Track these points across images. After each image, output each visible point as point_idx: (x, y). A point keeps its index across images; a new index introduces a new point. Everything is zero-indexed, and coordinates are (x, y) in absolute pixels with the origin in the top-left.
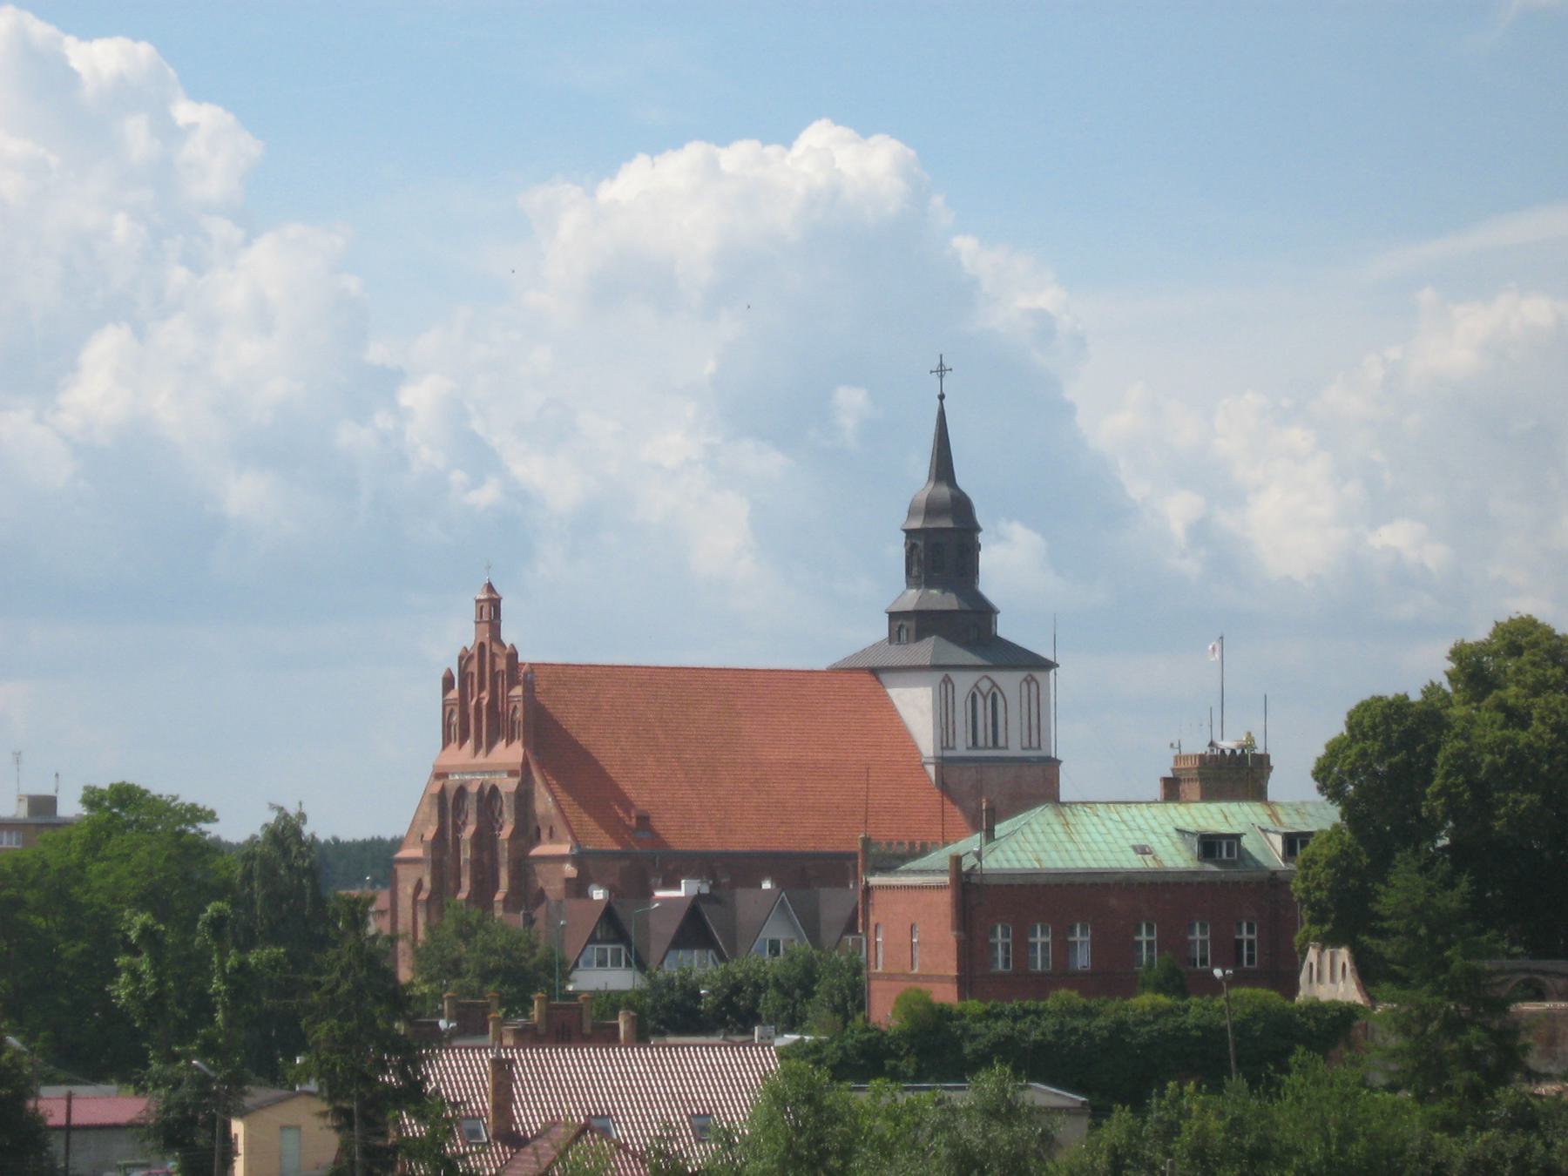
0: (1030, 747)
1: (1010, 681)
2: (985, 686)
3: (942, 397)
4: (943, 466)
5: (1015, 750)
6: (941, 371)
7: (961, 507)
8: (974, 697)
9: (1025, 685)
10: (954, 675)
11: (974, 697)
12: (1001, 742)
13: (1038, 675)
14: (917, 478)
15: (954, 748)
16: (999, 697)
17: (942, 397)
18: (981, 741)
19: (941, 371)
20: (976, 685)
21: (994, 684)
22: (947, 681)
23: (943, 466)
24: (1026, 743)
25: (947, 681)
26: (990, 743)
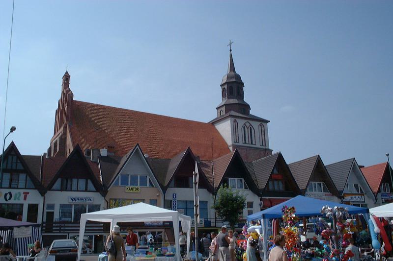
0: (262, 145)
1: (255, 125)
2: (248, 125)
3: (231, 50)
5: (258, 146)
6: (230, 44)
7: (238, 77)
8: (244, 129)
9: (260, 127)
10: (238, 120)
12: (254, 143)
14: (226, 70)
17: (231, 50)
18: (247, 142)
19: (230, 44)
20: (245, 124)
21: (251, 125)
24: (261, 144)
25: (235, 121)
26: (250, 143)
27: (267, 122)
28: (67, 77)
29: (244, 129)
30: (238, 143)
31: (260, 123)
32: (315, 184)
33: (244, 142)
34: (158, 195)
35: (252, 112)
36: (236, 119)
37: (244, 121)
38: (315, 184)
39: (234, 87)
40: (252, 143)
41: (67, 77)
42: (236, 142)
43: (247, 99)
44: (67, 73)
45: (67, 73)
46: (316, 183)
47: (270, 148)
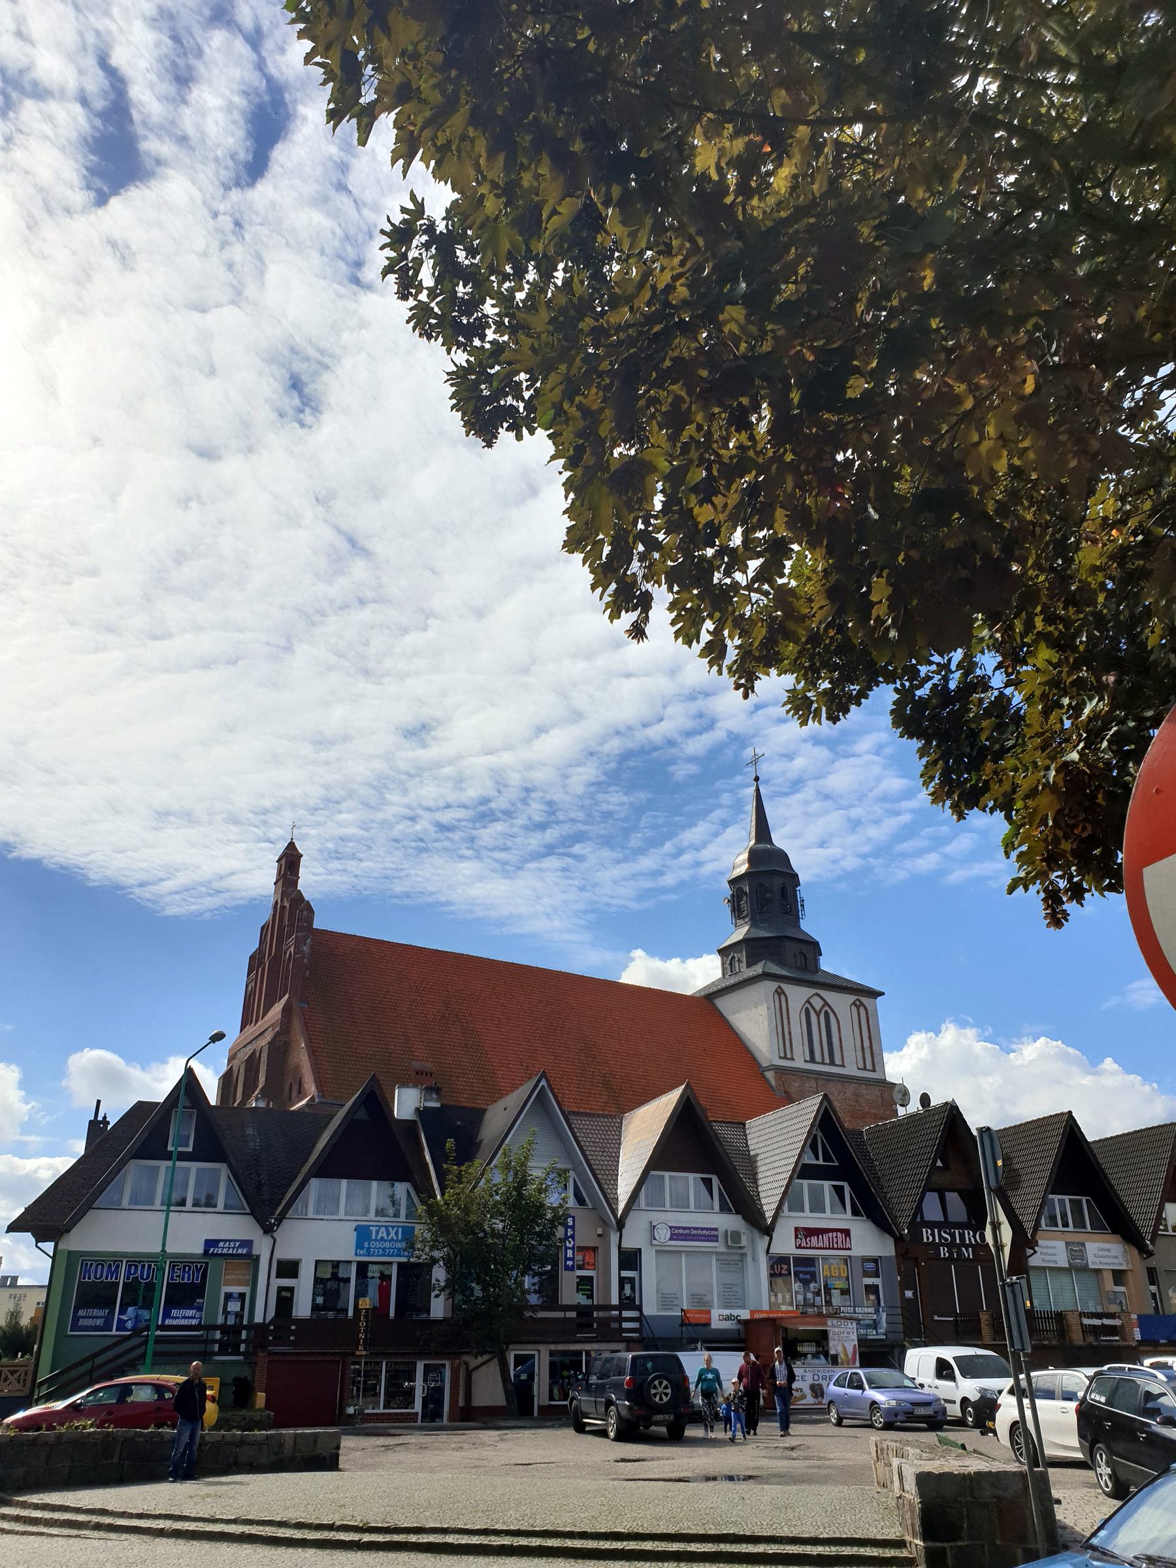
0: (865, 1069)
1: (841, 1003)
2: (817, 1003)
4: (763, 830)
5: (851, 1070)
10: (787, 988)
12: (838, 1061)
13: (864, 1000)
15: (792, 1059)
18: (818, 1058)
20: (808, 1001)
21: (826, 1004)
22: (780, 992)
23: (763, 830)
24: (861, 1066)
25: (780, 992)
26: (827, 1061)
27: (876, 994)
29: (807, 1011)
30: (792, 1059)
31: (853, 998)
32: (1062, 1202)
34: (600, 1231)
35: (827, 964)
36: (783, 986)
38: (1062, 1202)
42: (785, 1058)
43: (809, 925)
44: (291, 846)
45: (291, 846)
46: (1066, 1198)
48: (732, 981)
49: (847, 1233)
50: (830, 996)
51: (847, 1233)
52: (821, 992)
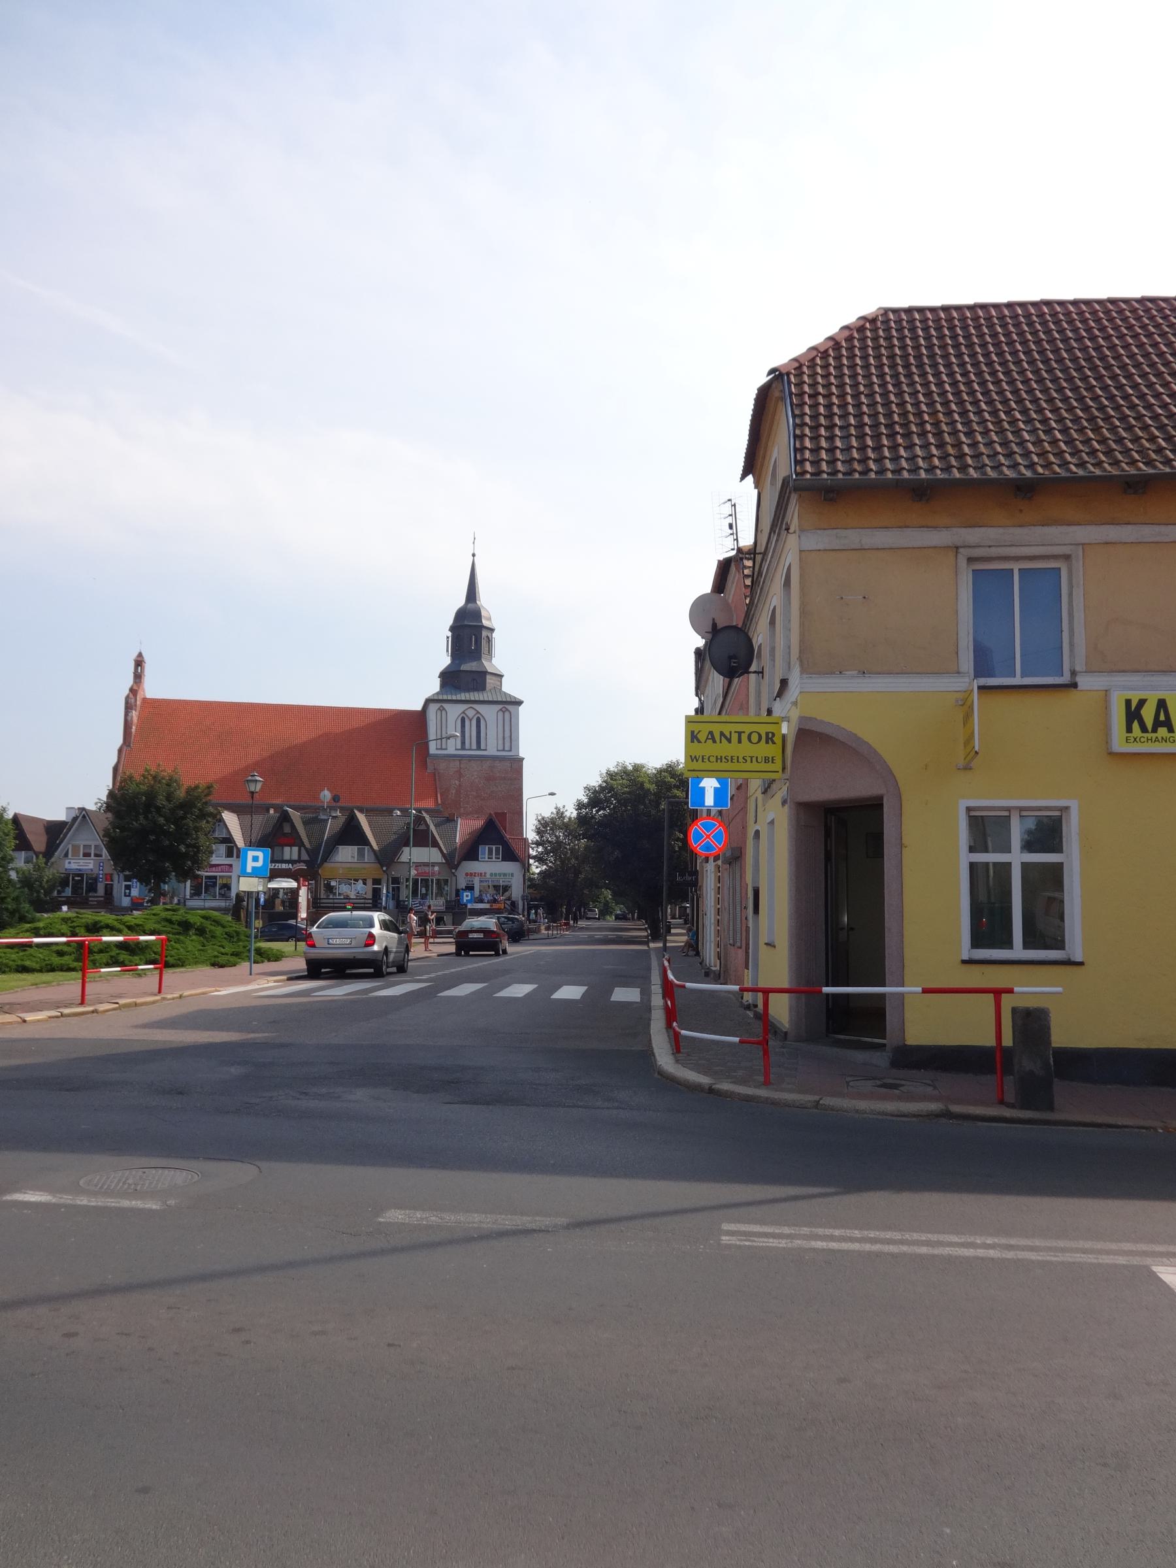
2: (471, 713)
3: (474, 555)
7: (477, 614)
8: (463, 720)
9: (501, 714)
10: (445, 705)
11: (463, 720)
13: (509, 707)
14: (460, 601)
16: (482, 722)
17: (474, 555)
22: (442, 709)
25: (442, 709)
26: (474, 747)
27: (520, 703)
28: (139, 663)
31: (500, 706)
33: (459, 746)
37: (461, 708)
39: (469, 633)
40: (479, 748)
41: (139, 663)
44: (140, 655)
45: (140, 655)
47: (521, 755)
48: (440, 697)
49: (231, 866)
50: (481, 708)
51: (231, 866)
52: (474, 706)
